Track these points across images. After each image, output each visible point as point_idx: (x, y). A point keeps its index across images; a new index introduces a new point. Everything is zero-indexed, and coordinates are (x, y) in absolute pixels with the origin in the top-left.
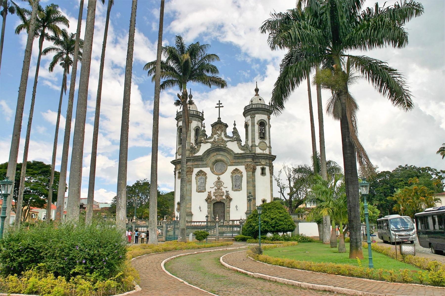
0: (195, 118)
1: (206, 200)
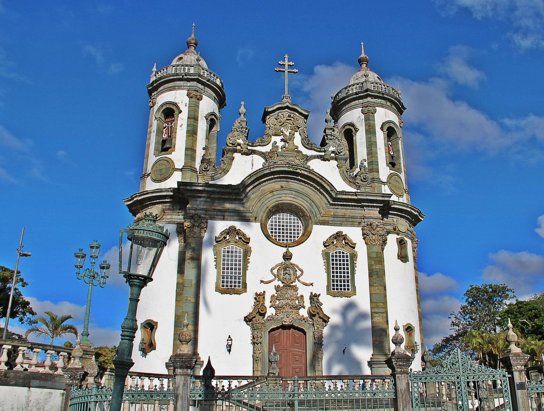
1: (248, 320)
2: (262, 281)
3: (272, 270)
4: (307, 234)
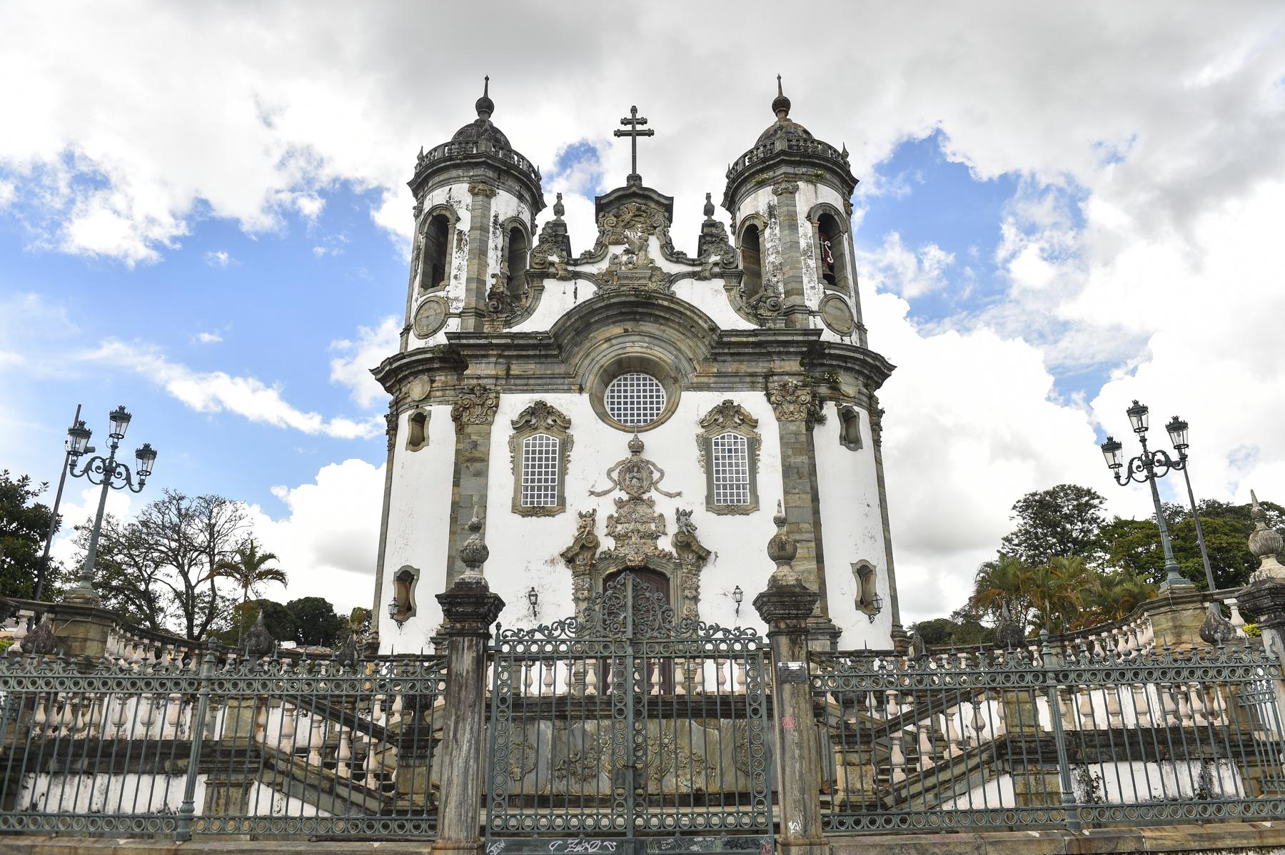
0: (510, 183)
1: (569, 558)
2: (592, 493)
3: (609, 474)
4: (671, 411)
